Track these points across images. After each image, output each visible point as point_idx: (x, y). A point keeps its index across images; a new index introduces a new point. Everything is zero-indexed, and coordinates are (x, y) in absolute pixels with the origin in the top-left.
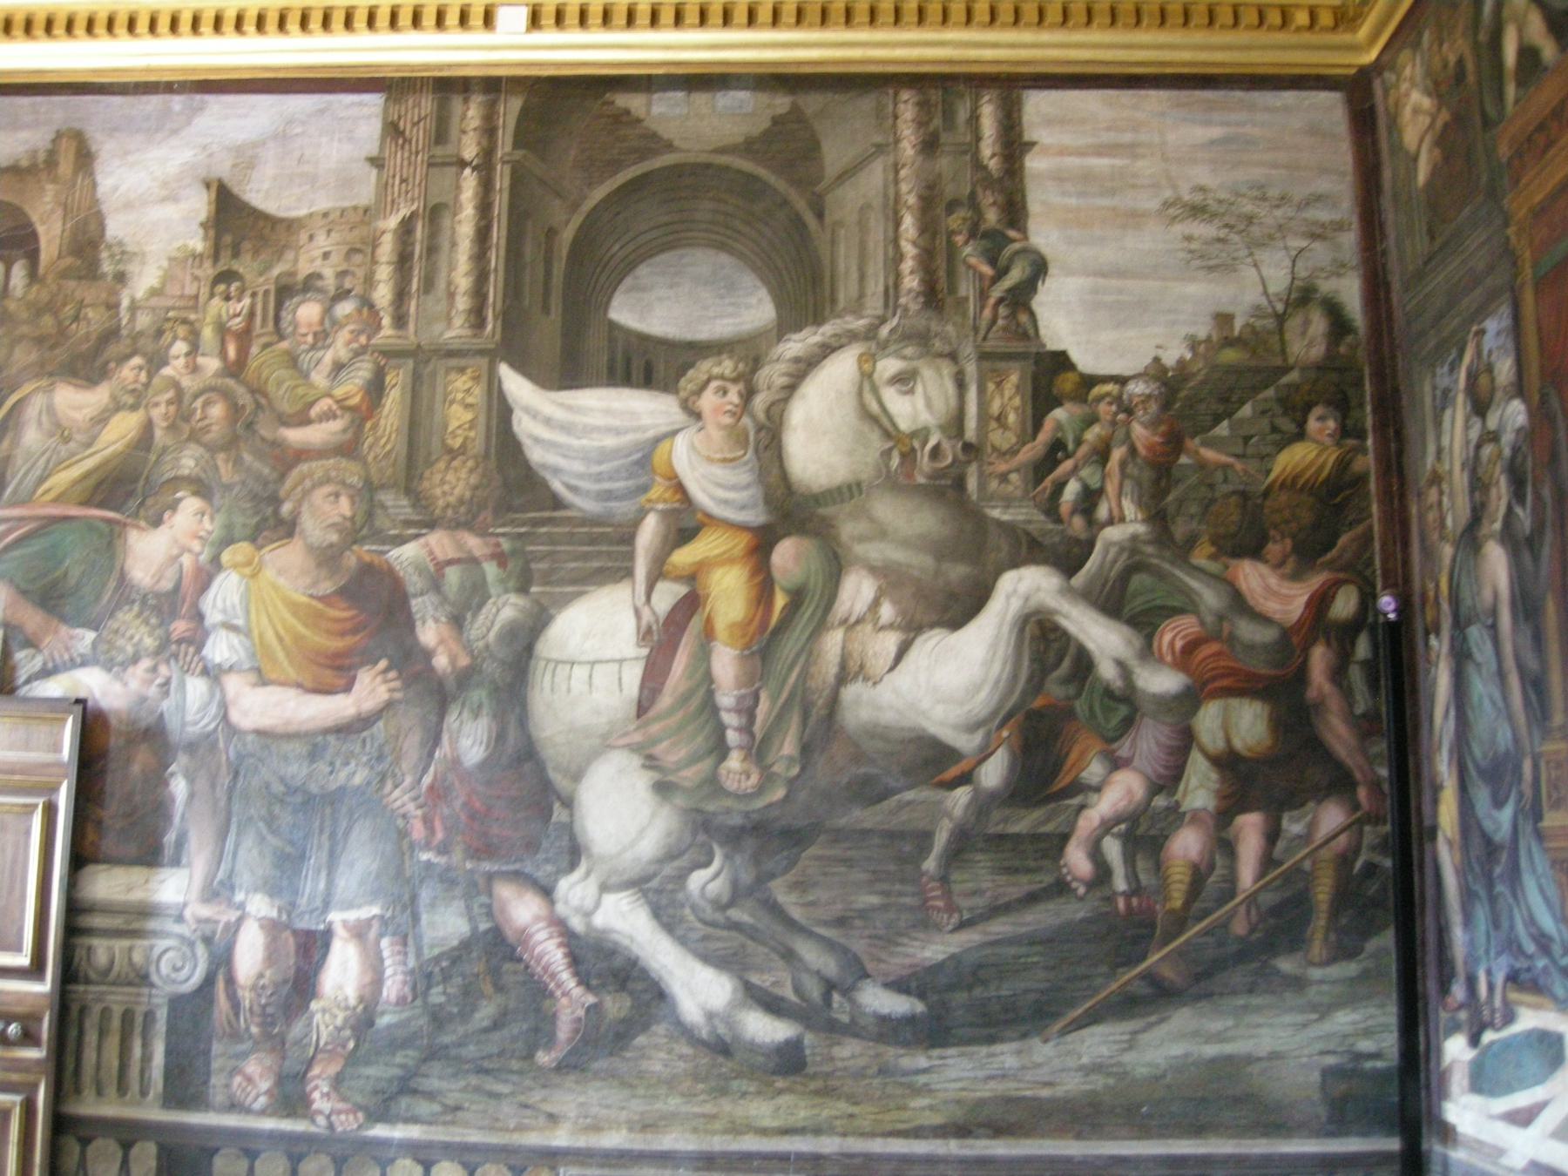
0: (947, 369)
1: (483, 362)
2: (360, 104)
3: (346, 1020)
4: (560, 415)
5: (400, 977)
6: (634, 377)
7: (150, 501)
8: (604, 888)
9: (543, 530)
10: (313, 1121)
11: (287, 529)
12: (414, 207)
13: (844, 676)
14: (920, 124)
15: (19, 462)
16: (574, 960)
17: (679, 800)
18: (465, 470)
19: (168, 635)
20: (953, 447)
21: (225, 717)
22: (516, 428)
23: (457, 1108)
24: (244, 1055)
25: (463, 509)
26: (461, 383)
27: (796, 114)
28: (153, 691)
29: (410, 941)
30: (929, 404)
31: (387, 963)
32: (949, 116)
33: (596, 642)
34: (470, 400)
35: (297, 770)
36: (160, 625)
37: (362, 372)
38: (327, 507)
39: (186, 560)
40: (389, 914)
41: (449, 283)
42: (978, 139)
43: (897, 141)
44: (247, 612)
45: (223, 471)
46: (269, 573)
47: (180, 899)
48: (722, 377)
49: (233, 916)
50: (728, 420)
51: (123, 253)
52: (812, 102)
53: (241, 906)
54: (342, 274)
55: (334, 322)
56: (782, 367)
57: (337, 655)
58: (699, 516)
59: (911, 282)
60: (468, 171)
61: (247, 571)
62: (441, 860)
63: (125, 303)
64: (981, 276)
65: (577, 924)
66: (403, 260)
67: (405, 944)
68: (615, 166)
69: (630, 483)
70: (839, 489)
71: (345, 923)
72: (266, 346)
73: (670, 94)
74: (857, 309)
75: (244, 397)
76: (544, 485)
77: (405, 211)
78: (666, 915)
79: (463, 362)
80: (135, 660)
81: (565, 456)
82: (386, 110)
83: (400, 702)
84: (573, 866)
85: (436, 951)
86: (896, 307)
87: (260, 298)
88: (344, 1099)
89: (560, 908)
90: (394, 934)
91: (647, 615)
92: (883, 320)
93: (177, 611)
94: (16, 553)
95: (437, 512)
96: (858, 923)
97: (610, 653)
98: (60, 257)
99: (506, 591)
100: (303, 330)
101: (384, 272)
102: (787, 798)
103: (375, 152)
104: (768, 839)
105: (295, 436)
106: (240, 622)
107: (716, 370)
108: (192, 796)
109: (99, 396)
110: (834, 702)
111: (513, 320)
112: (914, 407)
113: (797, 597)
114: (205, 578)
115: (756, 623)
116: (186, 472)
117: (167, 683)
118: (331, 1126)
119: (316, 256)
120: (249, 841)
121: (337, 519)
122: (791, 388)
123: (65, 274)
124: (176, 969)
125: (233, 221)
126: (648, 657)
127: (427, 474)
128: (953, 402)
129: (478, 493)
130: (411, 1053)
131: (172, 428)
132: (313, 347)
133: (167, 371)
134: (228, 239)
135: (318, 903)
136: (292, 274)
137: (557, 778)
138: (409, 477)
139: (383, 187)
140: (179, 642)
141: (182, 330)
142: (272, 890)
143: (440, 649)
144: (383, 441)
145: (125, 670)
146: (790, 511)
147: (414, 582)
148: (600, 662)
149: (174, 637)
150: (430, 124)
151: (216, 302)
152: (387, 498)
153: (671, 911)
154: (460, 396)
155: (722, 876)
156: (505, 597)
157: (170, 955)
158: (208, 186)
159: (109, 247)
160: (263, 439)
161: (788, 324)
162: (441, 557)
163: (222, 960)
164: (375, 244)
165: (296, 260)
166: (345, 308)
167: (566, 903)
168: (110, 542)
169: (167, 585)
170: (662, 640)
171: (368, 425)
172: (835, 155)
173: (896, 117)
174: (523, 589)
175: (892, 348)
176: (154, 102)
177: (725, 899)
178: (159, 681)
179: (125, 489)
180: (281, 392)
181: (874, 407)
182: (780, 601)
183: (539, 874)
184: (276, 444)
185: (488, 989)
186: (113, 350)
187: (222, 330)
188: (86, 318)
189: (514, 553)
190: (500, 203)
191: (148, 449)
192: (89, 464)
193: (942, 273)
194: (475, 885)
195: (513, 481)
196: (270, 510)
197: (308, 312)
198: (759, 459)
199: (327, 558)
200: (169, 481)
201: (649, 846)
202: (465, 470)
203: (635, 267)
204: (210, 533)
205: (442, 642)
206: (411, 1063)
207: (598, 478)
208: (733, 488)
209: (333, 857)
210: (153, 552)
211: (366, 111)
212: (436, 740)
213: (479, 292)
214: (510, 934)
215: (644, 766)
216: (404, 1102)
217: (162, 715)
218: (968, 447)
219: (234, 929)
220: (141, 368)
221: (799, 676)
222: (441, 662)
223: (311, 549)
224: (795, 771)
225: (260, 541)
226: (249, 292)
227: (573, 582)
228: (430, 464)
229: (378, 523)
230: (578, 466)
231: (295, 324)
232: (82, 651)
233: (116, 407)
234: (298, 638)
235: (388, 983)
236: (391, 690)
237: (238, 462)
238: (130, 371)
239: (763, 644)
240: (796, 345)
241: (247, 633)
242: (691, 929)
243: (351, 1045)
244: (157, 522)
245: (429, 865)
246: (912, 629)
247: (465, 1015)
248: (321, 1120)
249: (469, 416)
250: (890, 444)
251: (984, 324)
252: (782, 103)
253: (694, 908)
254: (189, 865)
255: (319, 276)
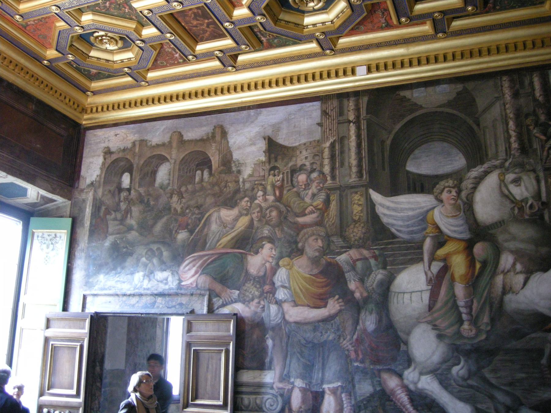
0: (532, 176)
1: (363, 189)
2: (313, 106)
4: (392, 205)
5: (349, 407)
6: (417, 189)
7: (254, 246)
8: (421, 374)
9: (389, 246)
11: (301, 252)
12: (334, 139)
13: (505, 292)
14: (511, 88)
15: (211, 235)
16: (412, 400)
17: (447, 341)
18: (360, 227)
19: (263, 290)
20: (538, 204)
21: (284, 318)
22: (377, 211)
25: (361, 241)
26: (356, 197)
27: (465, 90)
28: (259, 310)
29: (352, 394)
30: (527, 189)
31: (345, 402)
32: (522, 84)
33: (412, 284)
34: (360, 203)
35: (309, 335)
36: (260, 287)
37: (322, 196)
38: (314, 244)
39: (268, 265)
40: (344, 385)
41: (349, 163)
42: (534, 90)
43: (504, 95)
44: (289, 281)
45: (278, 234)
46: (295, 268)
47: (272, 381)
48: (449, 187)
49: (290, 387)
50: (453, 202)
51: (239, 163)
52: (470, 86)
53: (293, 383)
54: (312, 164)
55: (311, 180)
56: (470, 181)
57: (321, 294)
58: (446, 237)
59: (515, 145)
60: (352, 124)
61: (288, 267)
62: (362, 365)
63: (241, 180)
64: (541, 140)
65: (412, 387)
66: (332, 157)
67: (350, 396)
68: (403, 116)
69: (419, 227)
70: (496, 223)
71: (329, 388)
72: (289, 190)
73: (419, 89)
74: (496, 157)
75: (283, 208)
76: (389, 230)
77: (331, 140)
78: (445, 383)
79: (356, 190)
80: (253, 300)
81: (395, 220)
82: (321, 106)
83: (344, 310)
84: (409, 366)
85: (362, 398)
86: (510, 155)
87: (285, 174)
89: (405, 381)
90: (346, 392)
91: (429, 273)
92: (506, 160)
93: (266, 283)
94: (212, 266)
95: (352, 242)
96: (518, 384)
97: (417, 289)
98: (219, 167)
99: (378, 269)
100: (301, 184)
101: (326, 162)
102: (486, 339)
103: (319, 121)
104: (479, 354)
105: (301, 220)
106: (287, 285)
107: (447, 184)
108: (274, 345)
109: (235, 212)
110: (501, 301)
111: (372, 174)
112: (521, 190)
113: (484, 264)
114: (274, 271)
115: (470, 274)
116: (266, 235)
117: (264, 307)
119: (303, 158)
120: (294, 361)
121: (318, 247)
122: (475, 188)
123: (220, 173)
124: (271, 406)
125: (274, 149)
126: (431, 289)
127: (347, 230)
128: (536, 187)
129: (366, 235)
131: (260, 220)
132: (305, 189)
133: (257, 202)
134: (273, 155)
135: (319, 382)
136: (295, 165)
137: (401, 334)
138: (341, 232)
139: (324, 132)
140: (267, 293)
141: (260, 188)
142: (303, 377)
143: (357, 290)
144: (331, 220)
145: (249, 303)
146: (478, 232)
147: (346, 268)
148: (414, 292)
149: (265, 291)
150: (337, 110)
151: (271, 177)
152: (334, 239)
153: (446, 382)
154: (356, 201)
155: (464, 368)
156: (378, 271)
157: (269, 400)
158: (265, 139)
159: (234, 162)
160: (290, 222)
161: (471, 166)
162: (354, 258)
164: (322, 153)
165: (296, 161)
166: (314, 175)
167: (407, 379)
168: (242, 260)
169: (262, 274)
170: (436, 283)
171: (326, 214)
172: (481, 103)
173: (502, 86)
174: (384, 268)
175: (510, 171)
176: (245, 113)
177: (466, 376)
178: (261, 306)
179: (246, 242)
180: (295, 205)
181: (506, 192)
182: (478, 266)
183: (397, 369)
184: (295, 223)
186: (238, 196)
187: (274, 186)
188: (229, 186)
189: (380, 255)
190: (364, 134)
191: (252, 229)
192: (233, 234)
193: (526, 141)
194: (374, 373)
195: (378, 231)
196: (294, 246)
197: (302, 178)
198: (465, 215)
199: (315, 261)
200: (260, 238)
201: (436, 358)
202: (360, 227)
203: (413, 151)
204: (274, 255)
205: (357, 288)
207: (408, 226)
208: (457, 226)
209: (324, 365)
210: (256, 263)
211: (315, 107)
212: (357, 323)
213: (360, 166)
214: (388, 391)
215: (433, 329)
217: (262, 318)
218: (543, 203)
219: (291, 391)
220: (248, 201)
221: (487, 294)
222: (357, 295)
223: (309, 258)
224: (489, 328)
225: (292, 257)
226: (281, 173)
227: (402, 264)
228: (348, 226)
229: (332, 248)
230: (400, 223)
231: (298, 182)
232: (235, 297)
233: (241, 215)
234: (307, 289)
235: (345, 409)
236: (340, 306)
237: (282, 230)
238: (244, 203)
239: (473, 282)
240: (474, 173)
241: (290, 289)
242: (455, 388)
244: (257, 253)
245: (357, 367)
246: (529, 273)
249: (360, 209)
250: (514, 205)
251: (544, 158)
252: (460, 87)
253: (454, 380)
254: (274, 369)
255: (305, 165)
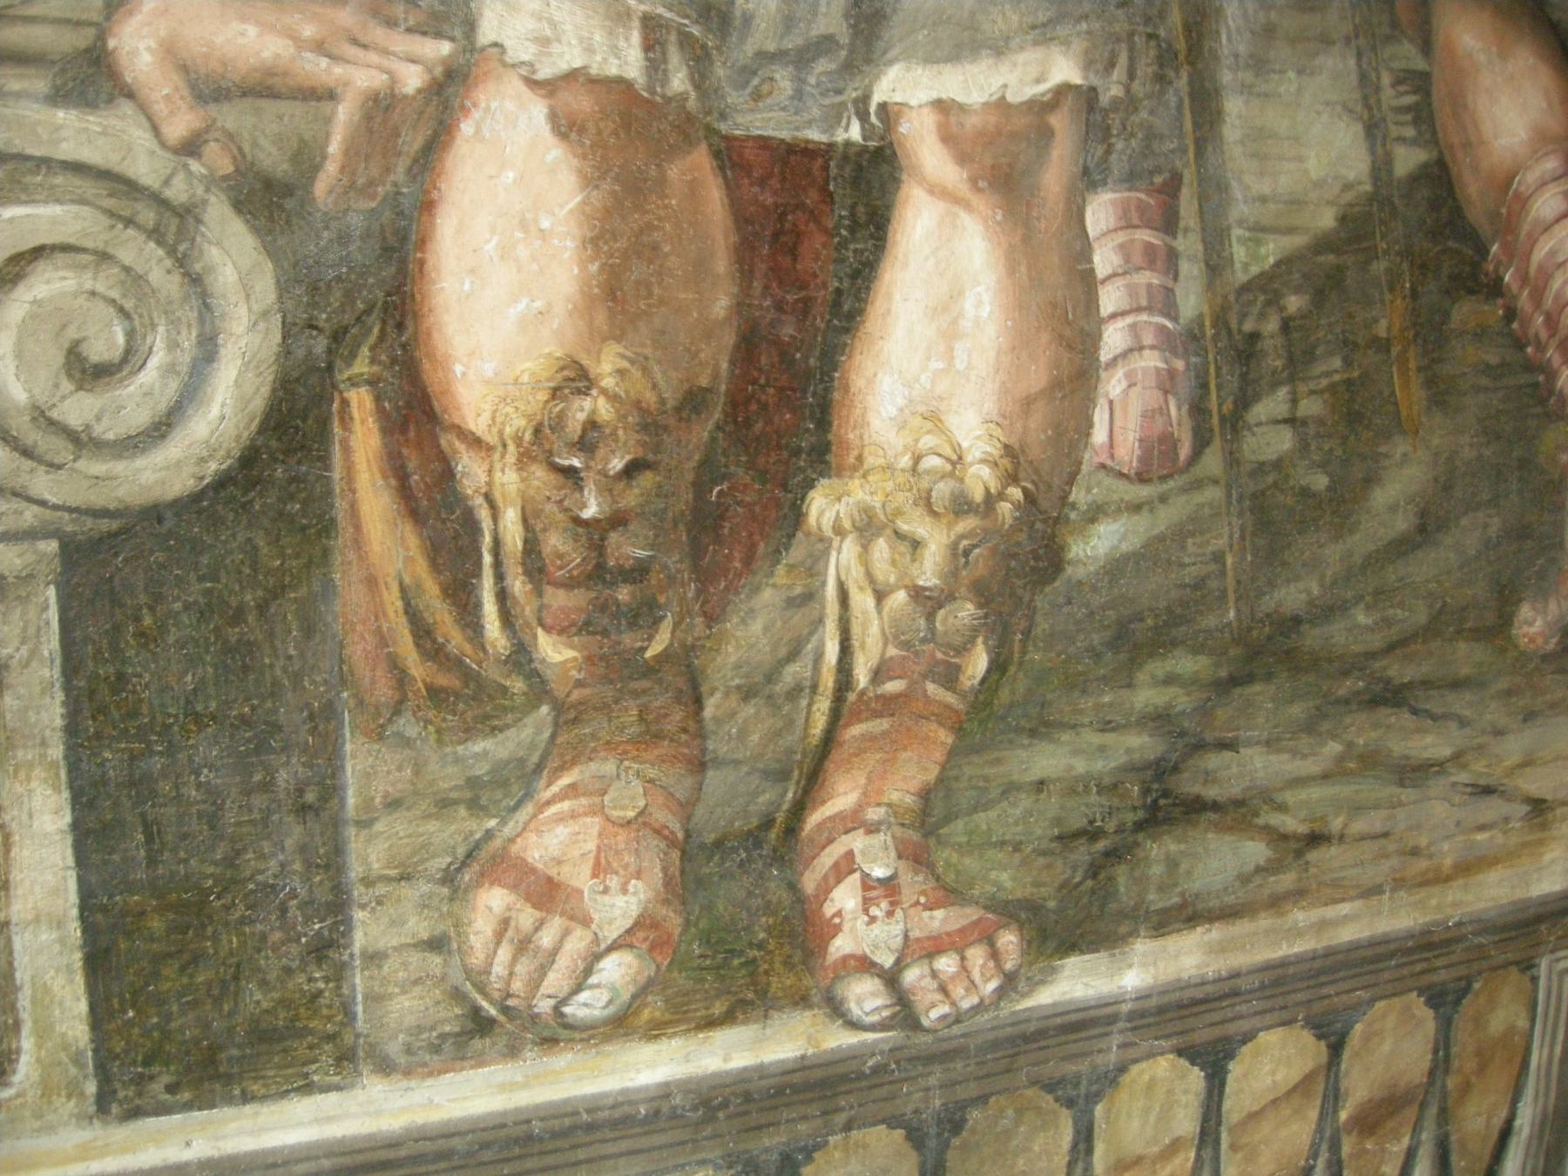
3: (958, 554)
5: (1151, 361)
10: (836, 1009)
23: (1316, 839)
24: (516, 783)
31: (1110, 299)
40: (1112, 90)
67: (1169, 224)
71: (941, 106)
85: (1272, 250)
88: (950, 893)
90: (1131, 178)
118: (905, 1013)
124: (88, 373)
130: (1186, 664)
163: (363, 306)
185: (1411, 395)
206: (1182, 701)
216: (1158, 850)
219: (421, 133)
235: (1113, 385)
243: (978, 663)
247: (1340, 506)
248: (865, 997)
